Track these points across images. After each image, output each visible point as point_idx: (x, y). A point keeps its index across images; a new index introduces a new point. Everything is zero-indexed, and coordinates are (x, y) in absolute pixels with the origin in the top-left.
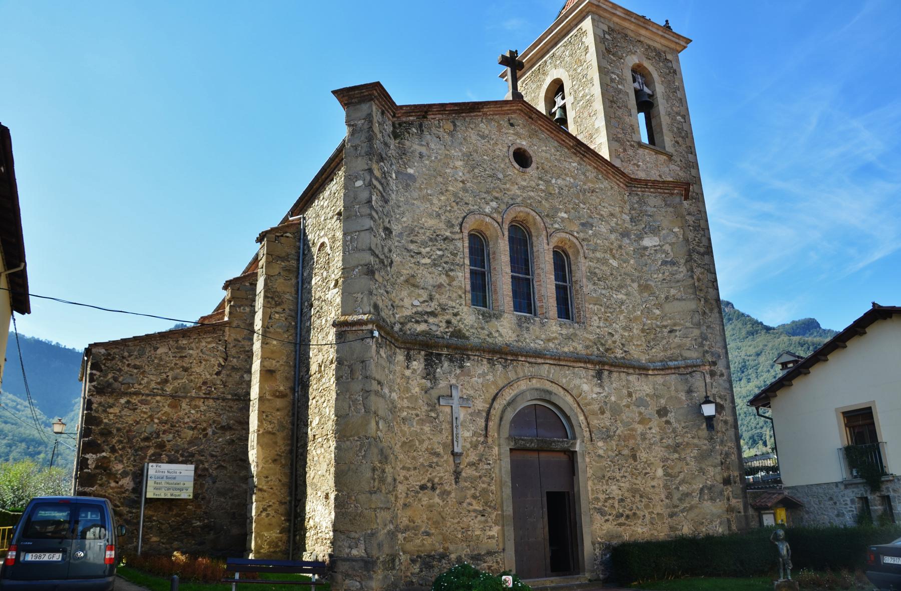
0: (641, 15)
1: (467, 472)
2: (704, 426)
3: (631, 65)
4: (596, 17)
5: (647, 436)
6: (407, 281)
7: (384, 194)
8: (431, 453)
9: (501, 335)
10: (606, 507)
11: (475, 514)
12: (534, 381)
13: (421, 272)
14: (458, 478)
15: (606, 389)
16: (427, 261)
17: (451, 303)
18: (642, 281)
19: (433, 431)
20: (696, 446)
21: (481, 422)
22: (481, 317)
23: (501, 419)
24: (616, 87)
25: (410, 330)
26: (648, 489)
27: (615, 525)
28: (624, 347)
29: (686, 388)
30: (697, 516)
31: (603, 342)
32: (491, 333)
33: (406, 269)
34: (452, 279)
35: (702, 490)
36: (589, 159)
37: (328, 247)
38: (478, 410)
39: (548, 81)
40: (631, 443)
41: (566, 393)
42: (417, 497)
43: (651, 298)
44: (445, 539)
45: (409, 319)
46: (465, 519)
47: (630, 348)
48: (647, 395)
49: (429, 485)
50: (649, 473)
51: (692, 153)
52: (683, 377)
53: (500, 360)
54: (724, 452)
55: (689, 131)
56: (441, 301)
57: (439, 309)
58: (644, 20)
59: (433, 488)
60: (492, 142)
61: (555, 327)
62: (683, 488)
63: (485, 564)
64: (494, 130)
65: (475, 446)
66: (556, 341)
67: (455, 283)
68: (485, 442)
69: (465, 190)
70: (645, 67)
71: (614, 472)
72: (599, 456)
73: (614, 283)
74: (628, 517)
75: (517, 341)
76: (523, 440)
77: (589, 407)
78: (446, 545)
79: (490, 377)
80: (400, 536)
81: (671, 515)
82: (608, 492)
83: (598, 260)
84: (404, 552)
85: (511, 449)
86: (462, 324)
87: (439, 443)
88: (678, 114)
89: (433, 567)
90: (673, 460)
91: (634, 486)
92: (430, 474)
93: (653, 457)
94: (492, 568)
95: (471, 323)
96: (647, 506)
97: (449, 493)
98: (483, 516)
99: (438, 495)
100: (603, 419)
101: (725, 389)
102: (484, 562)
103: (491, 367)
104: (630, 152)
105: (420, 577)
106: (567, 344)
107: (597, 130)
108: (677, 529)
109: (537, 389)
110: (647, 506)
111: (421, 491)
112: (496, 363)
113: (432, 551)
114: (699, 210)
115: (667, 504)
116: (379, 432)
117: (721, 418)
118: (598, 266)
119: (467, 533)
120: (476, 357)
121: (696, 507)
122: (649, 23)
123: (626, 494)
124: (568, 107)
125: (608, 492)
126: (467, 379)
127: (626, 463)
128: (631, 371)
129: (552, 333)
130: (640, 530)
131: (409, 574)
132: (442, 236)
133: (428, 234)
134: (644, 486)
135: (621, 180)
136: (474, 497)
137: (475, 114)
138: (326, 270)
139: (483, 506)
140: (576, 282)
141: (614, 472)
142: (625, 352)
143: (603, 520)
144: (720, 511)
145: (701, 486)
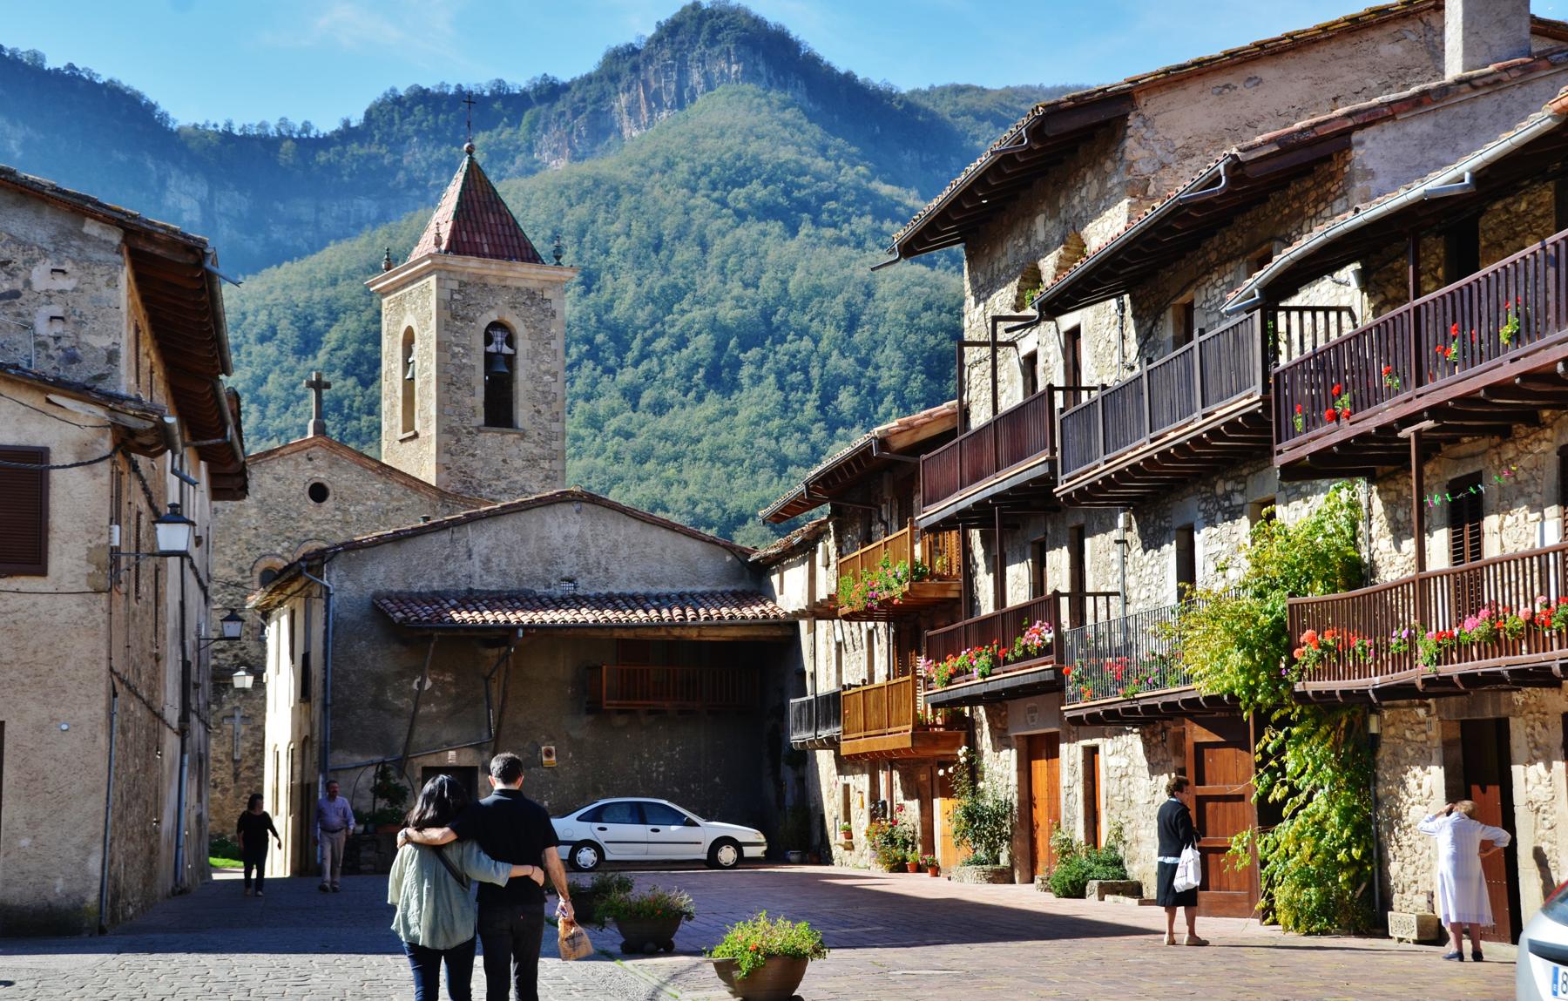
1: (245, 774)
4: (443, 274)
64: (291, 470)
88: (547, 372)
97: (228, 790)
104: (466, 441)
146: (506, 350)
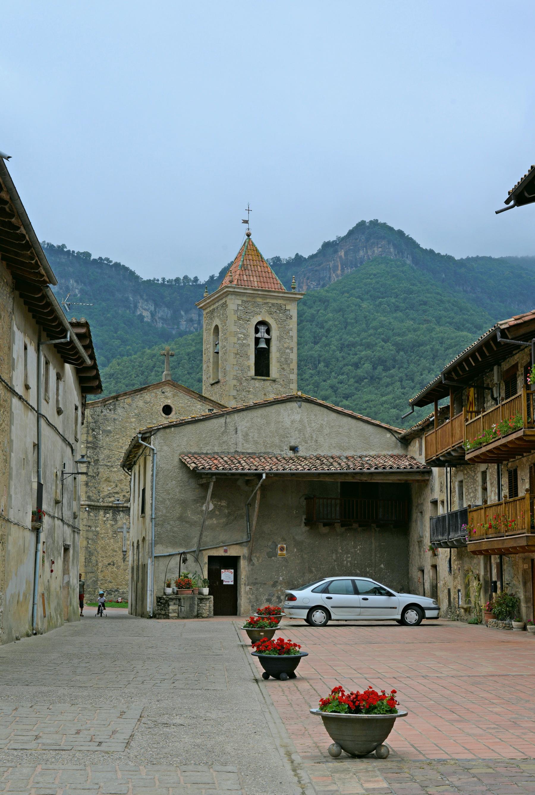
6: (106, 480)
24: (241, 342)
49: (112, 563)
59: (114, 565)
60: (151, 405)
87: (117, 547)
104: (245, 384)
146: (266, 336)
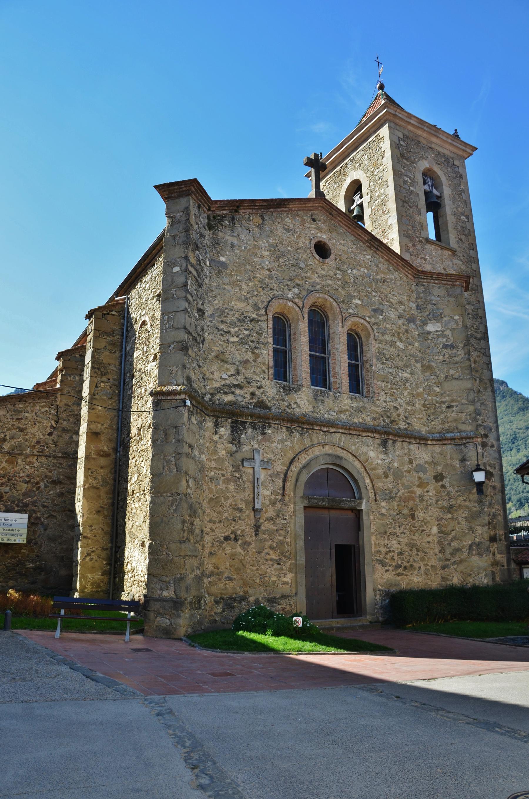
0: (432, 124)
1: (266, 526)
2: (475, 490)
3: (422, 169)
4: (393, 125)
5: (425, 498)
6: (217, 357)
7: (199, 279)
8: (234, 509)
9: (299, 406)
10: (387, 559)
11: (272, 563)
12: (327, 447)
13: (229, 349)
14: (258, 531)
15: (390, 456)
16: (235, 339)
17: (255, 377)
18: (425, 362)
19: (237, 489)
20: (467, 507)
21: (280, 483)
22: (281, 390)
23: (297, 480)
25: (218, 400)
26: (424, 544)
27: (394, 575)
28: (407, 419)
29: (460, 457)
30: (466, 568)
31: (389, 414)
32: (290, 405)
33: (217, 346)
34: (257, 356)
35: (470, 546)
36: (382, 252)
37: (149, 325)
38: (277, 472)
39: (348, 181)
40: (411, 504)
41: (355, 459)
42: (221, 546)
43: (433, 377)
44: (245, 584)
45: (218, 390)
46: (263, 567)
47: (413, 420)
48: (426, 462)
49: (232, 536)
50: (425, 530)
51: (473, 250)
52: (458, 447)
53: (297, 428)
54: (492, 514)
55: (471, 230)
56: (247, 375)
57: (245, 382)
58: (435, 129)
59: (236, 540)
60: (296, 235)
61: (346, 401)
62: (455, 544)
63: (280, 607)
64: (298, 225)
65: (273, 503)
66: (347, 413)
67: (259, 360)
68: (282, 500)
69: (271, 277)
70: (434, 171)
71: (394, 528)
72: (382, 514)
73: (400, 363)
74: (405, 568)
75: (313, 412)
76: (315, 499)
77: (374, 471)
78: (246, 589)
79: (288, 443)
80: (206, 580)
81: (444, 567)
82: (388, 546)
83: (387, 342)
84: (209, 595)
85: (304, 507)
86: (265, 396)
87: (242, 500)
88: (462, 214)
89: (234, 608)
90: (446, 520)
91: (412, 541)
92: (234, 527)
93: (430, 516)
94: (286, 610)
95: (273, 395)
96: (422, 559)
97: (250, 544)
98: (279, 564)
99: (240, 545)
100: (386, 482)
101: (495, 458)
102: (279, 605)
103: (289, 435)
104: (419, 247)
105: (222, 616)
106: (357, 416)
107: (390, 226)
108: (448, 580)
109: (329, 455)
110: (422, 559)
111: (225, 542)
112: (294, 431)
113: (233, 594)
114: (477, 301)
115: (440, 558)
116: (189, 490)
117: (490, 484)
118: (387, 348)
119: (264, 579)
120: (276, 426)
121: (465, 561)
122: (440, 132)
123: (405, 548)
124: (365, 205)
125: (388, 546)
126: (268, 444)
127: (405, 521)
128: (412, 441)
129: (344, 406)
130: (415, 580)
131: (213, 614)
132: (249, 318)
133: (236, 316)
134: (420, 541)
135: (410, 272)
136: (271, 548)
137: (282, 209)
138: (146, 345)
139: (279, 555)
140: (367, 361)
141: (394, 528)
142: (408, 424)
143: (384, 570)
144: (486, 564)
145: (470, 543)
